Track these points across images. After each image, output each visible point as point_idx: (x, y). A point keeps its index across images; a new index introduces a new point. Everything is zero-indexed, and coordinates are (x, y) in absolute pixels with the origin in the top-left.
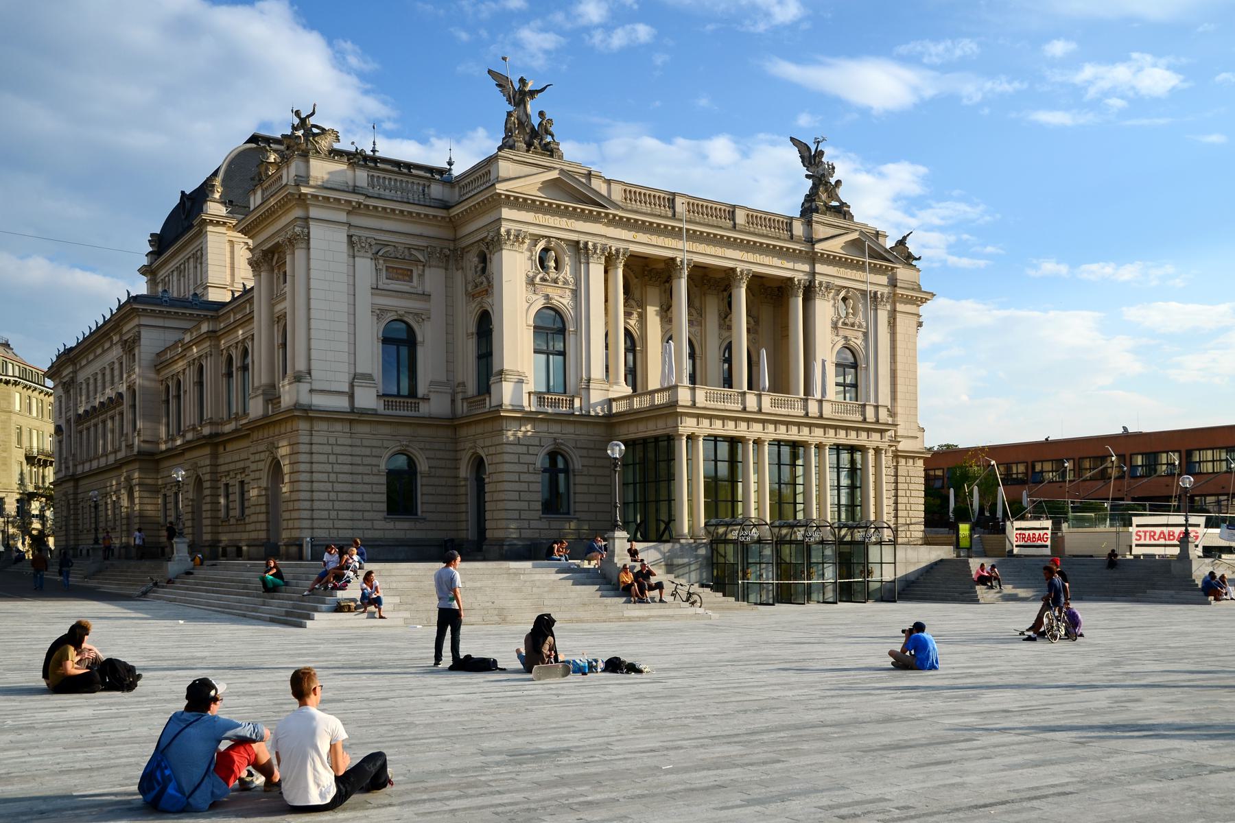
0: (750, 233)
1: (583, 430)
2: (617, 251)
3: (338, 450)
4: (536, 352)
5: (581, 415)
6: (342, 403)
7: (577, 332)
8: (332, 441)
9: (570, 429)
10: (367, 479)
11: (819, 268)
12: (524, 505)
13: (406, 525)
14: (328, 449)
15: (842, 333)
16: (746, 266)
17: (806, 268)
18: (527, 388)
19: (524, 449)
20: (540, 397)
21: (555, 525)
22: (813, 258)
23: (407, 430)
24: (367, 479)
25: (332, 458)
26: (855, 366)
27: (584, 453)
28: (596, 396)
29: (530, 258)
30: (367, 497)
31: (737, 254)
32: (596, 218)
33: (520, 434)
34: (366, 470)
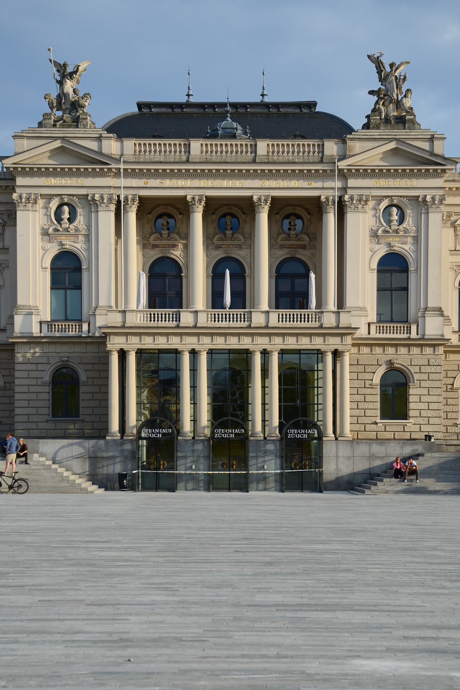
0: (274, 163)
1: (91, 349)
2: (126, 198)
5: (89, 337)
7: (89, 269)
9: (77, 348)
15: (382, 241)
16: (266, 192)
17: (338, 184)
18: (35, 320)
19: (34, 367)
20: (50, 324)
21: (60, 426)
28: (100, 321)
29: (46, 214)
31: (257, 183)
32: (102, 174)
33: (29, 355)
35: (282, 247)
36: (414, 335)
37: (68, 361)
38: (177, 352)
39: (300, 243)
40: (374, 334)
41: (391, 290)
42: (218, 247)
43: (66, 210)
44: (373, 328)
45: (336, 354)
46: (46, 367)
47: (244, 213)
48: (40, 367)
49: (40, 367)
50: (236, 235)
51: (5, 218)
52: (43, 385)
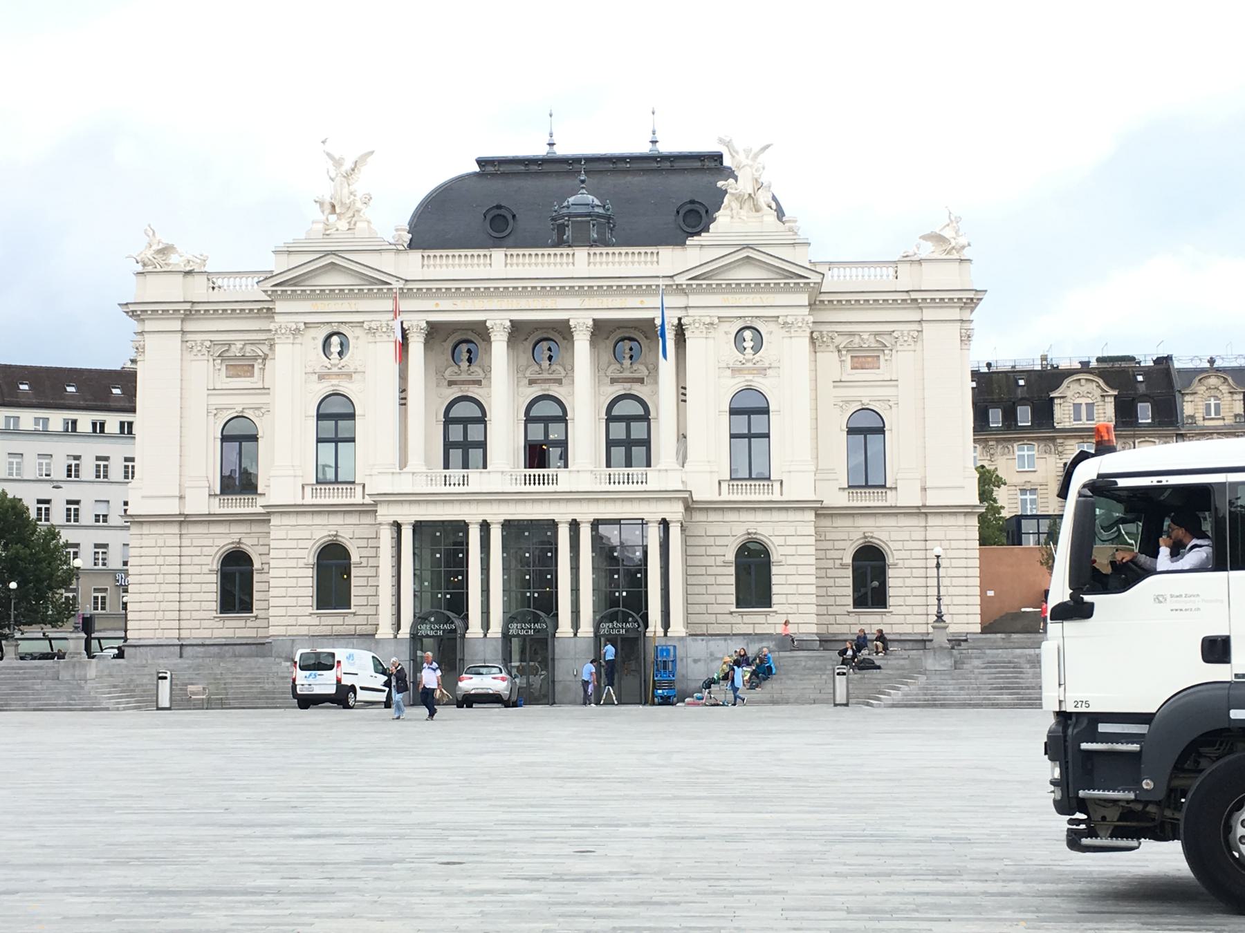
3: (165, 551)
4: (319, 441)
6: (172, 508)
8: (160, 543)
10: (196, 578)
11: (694, 300)
12: (293, 602)
13: (242, 623)
14: (156, 551)
19: (293, 544)
22: (680, 290)
23: (236, 529)
24: (196, 578)
25: (160, 560)
26: (765, 411)
27: (363, 543)
30: (196, 597)
34: (196, 569)
35: (614, 381)
36: (776, 497)
37: (336, 536)
38: (463, 526)
39: (636, 375)
40: (725, 496)
41: (750, 436)
42: (532, 382)
43: (335, 341)
44: (724, 486)
45: (665, 524)
46: (309, 544)
47: (564, 338)
48: (302, 544)
49: (302, 544)
50: (554, 367)
51: (266, 349)
52: (306, 566)
